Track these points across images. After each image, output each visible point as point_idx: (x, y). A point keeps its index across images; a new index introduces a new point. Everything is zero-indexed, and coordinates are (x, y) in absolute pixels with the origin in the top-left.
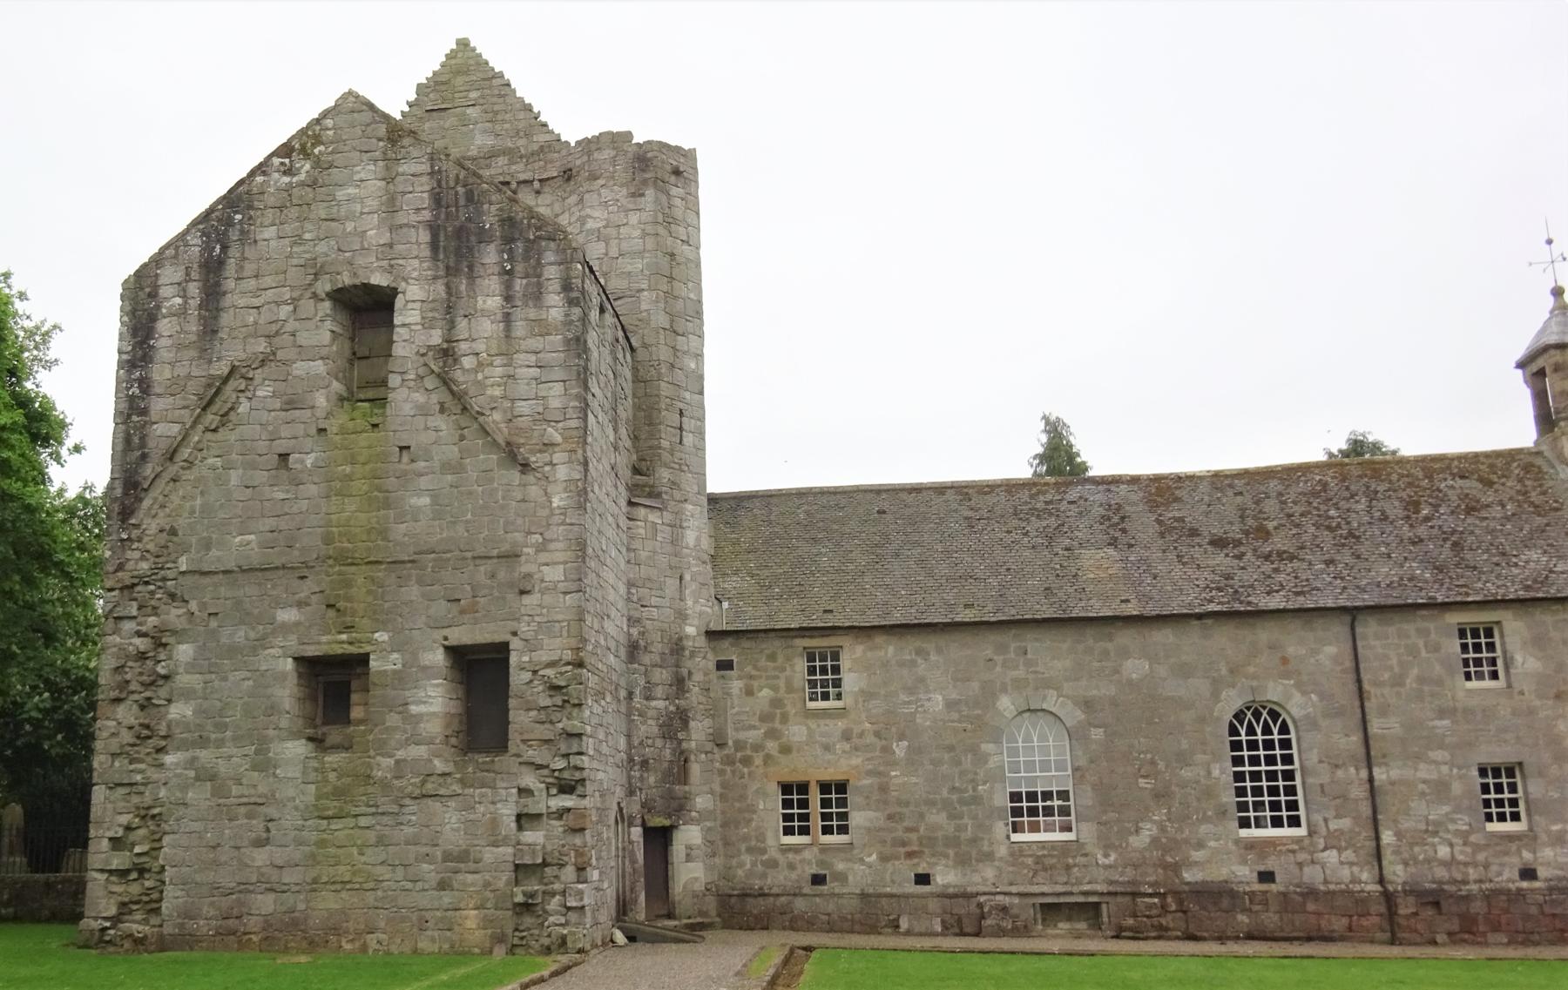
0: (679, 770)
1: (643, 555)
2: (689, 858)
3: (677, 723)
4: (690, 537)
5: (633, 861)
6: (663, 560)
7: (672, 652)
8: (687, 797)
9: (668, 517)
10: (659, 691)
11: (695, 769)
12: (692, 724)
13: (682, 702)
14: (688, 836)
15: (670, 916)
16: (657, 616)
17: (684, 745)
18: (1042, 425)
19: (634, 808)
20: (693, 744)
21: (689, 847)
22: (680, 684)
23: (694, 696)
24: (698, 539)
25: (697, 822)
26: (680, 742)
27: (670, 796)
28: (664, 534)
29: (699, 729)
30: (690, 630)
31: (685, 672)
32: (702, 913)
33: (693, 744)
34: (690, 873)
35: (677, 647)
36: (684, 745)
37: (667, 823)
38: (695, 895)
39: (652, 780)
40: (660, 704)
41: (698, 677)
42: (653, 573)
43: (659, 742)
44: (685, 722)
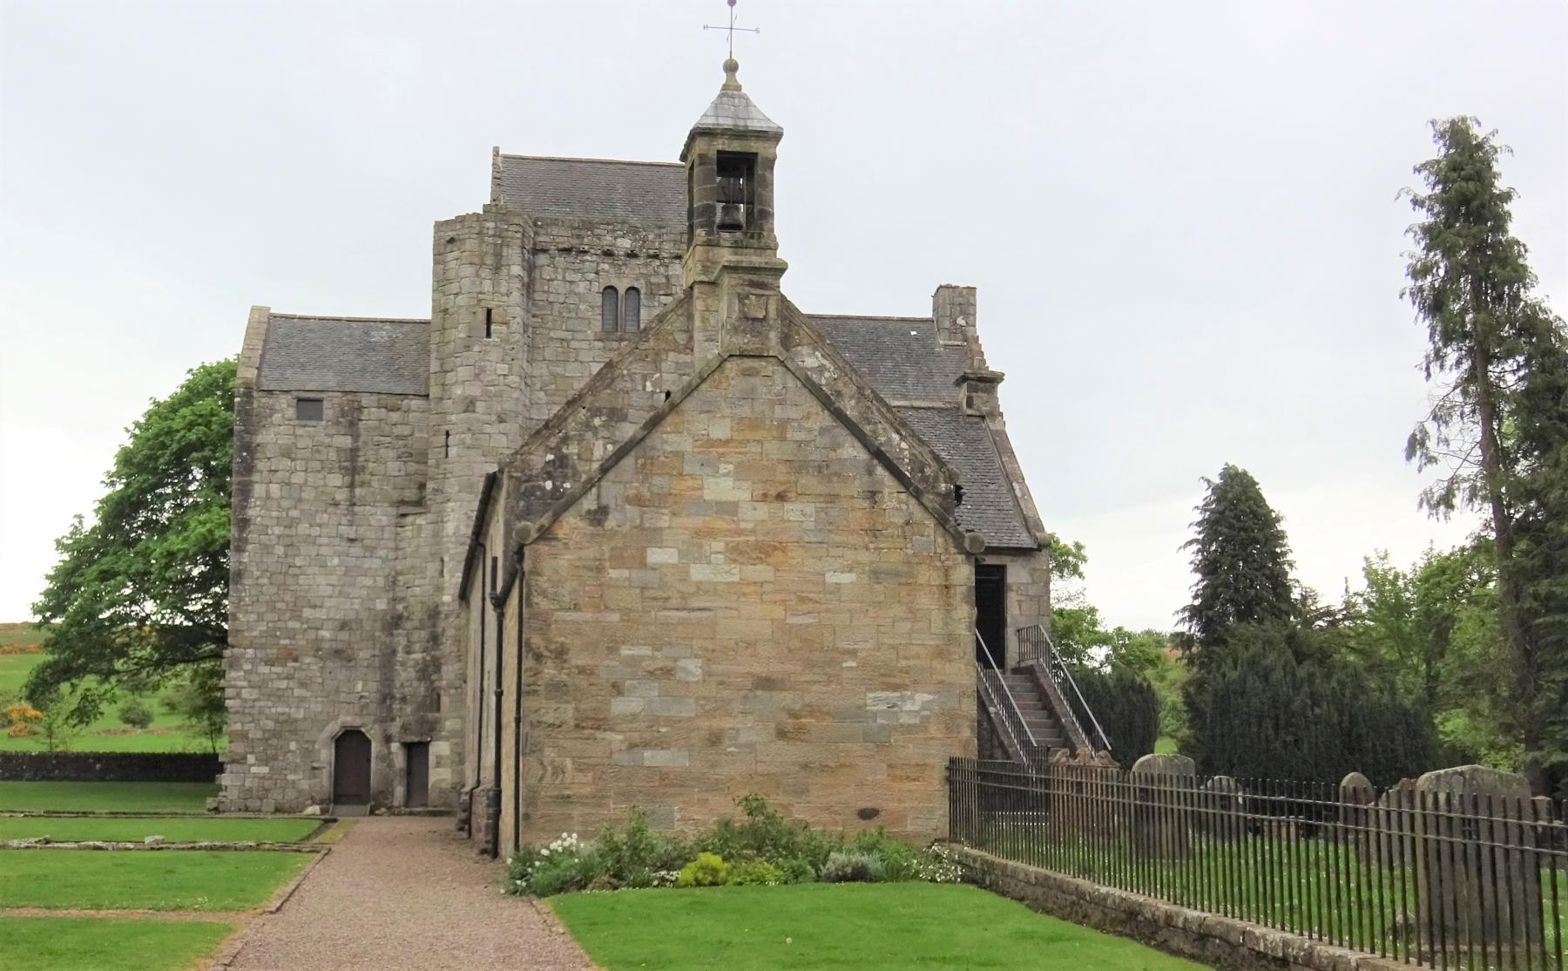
0: (433, 701)
1: (409, 550)
2: (438, 765)
3: (431, 669)
4: (450, 528)
5: (391, 765)
6: (425, 550)
7: (430, 617)
8: (437, 721)
9: (430, 517)
10: (417, 647)
11: (445, 701)
12: (444, 668)
13: (437, 653)
14: (439, 748)
15: (425, 805)
16: (418, 592)
17: (437, 684)
18: (1436, 151)
19: (395, 728)
20: (444, 683)
21: (439, 757)
22: (435, 639)
23: (448, 646)
24: (457, 528)
25: (447, 739)
26: (432, 682)
27: (422, 721)
28: (427, 531)
29: (449, 672)
30: (447, 598)
31: (439, 630)
32: (450, 805)
33: (444, 683)
34: (439, 776)
35: (434, 614)
36: (437, 684)
37: (416, 739)
38: (442, 791)
39: (409, 709)
40: (418, 656)
41: (450, 632)
42: (417, 562)
43: (415, 684)
44: (438, 669)
